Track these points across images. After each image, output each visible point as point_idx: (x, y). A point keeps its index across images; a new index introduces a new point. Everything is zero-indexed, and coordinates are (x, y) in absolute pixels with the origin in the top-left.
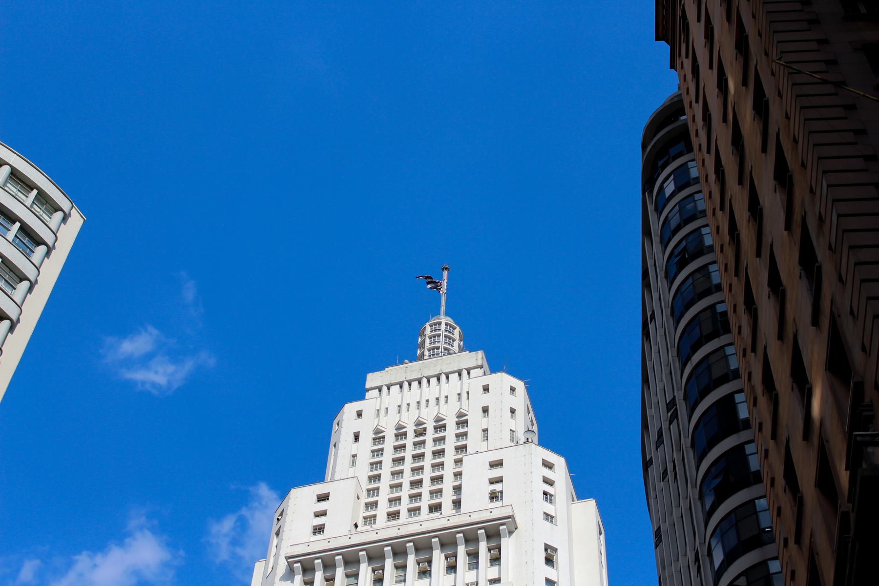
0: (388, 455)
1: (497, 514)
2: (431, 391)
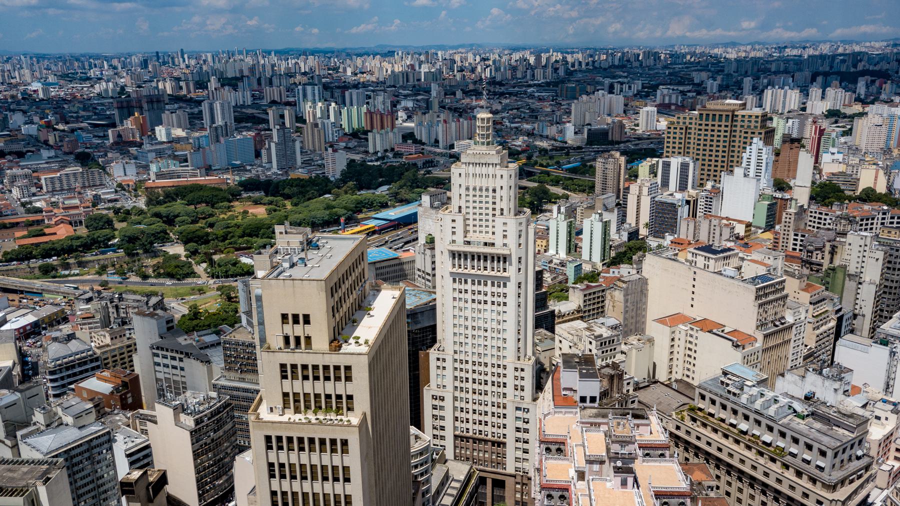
2: (484, 170)
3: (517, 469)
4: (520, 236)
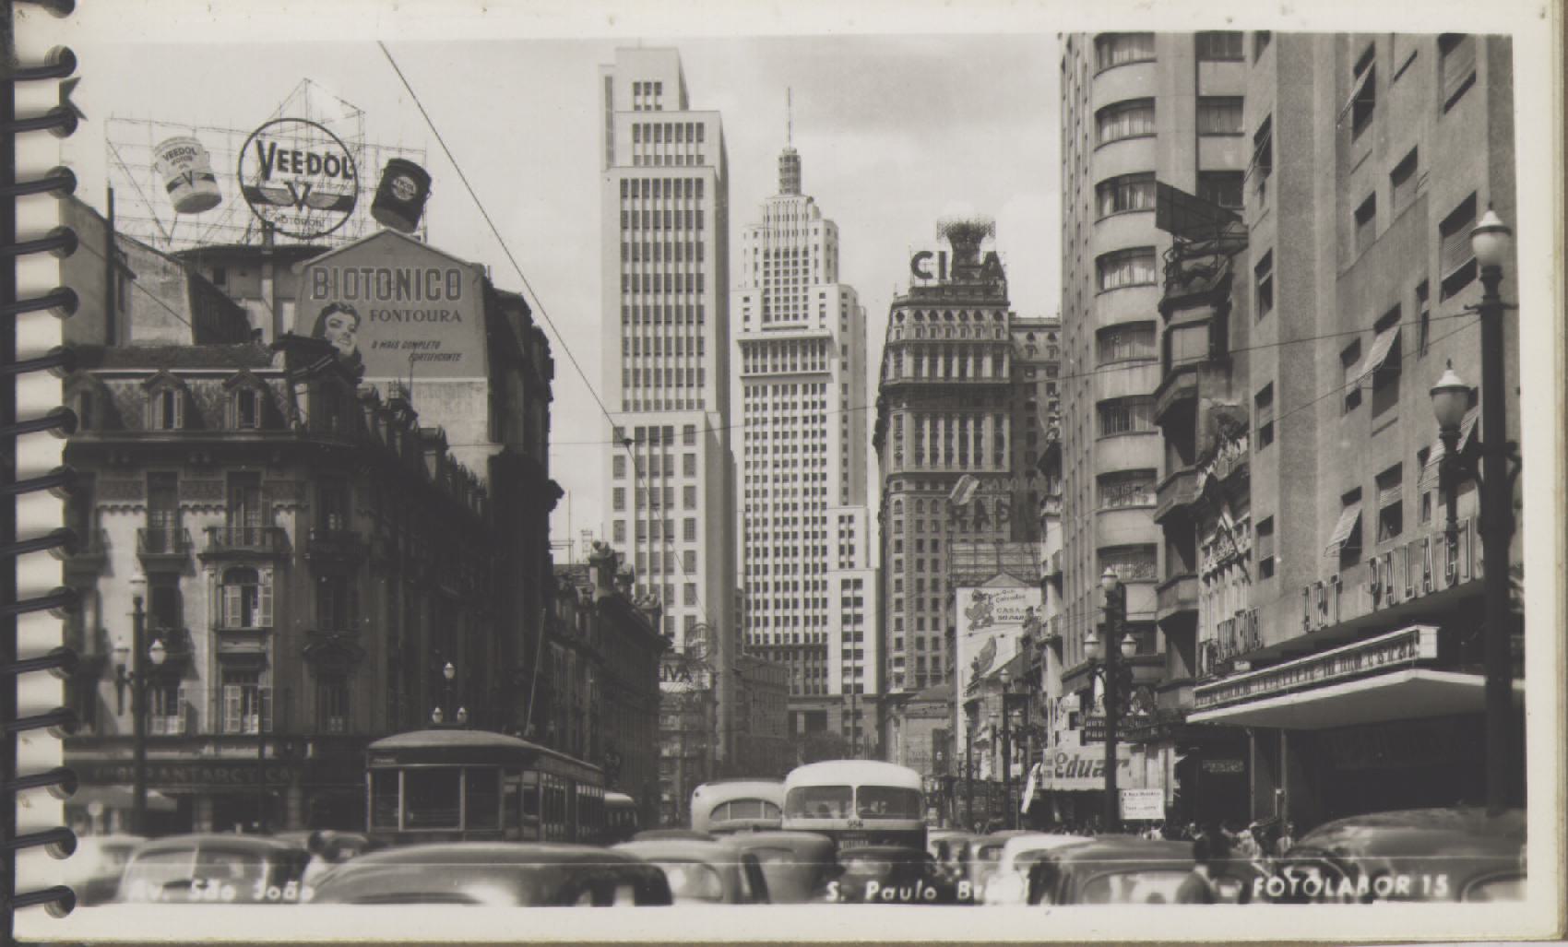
0: (772, 269)
1: (825, 333)
3: (846, 688)
4: (844, 315)
